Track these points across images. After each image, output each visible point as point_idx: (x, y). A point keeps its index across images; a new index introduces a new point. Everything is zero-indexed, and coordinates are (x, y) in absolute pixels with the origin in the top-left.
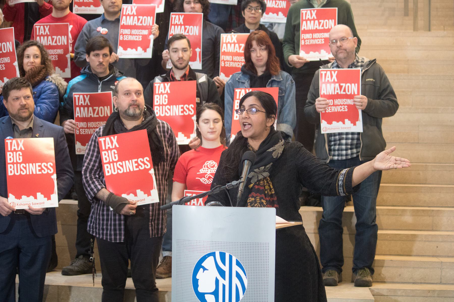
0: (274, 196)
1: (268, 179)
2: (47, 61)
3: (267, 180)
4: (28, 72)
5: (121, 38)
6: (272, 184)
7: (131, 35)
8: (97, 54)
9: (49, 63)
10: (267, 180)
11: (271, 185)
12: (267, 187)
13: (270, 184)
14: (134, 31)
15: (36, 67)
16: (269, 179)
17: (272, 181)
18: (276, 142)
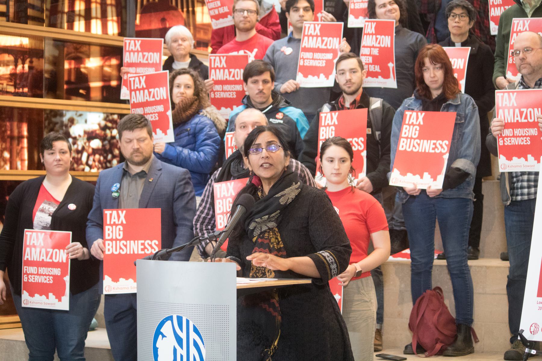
0: (283, 249)
1: (275, 230)
2: (202, 93)
3: (274, 231)
4: (178, 105)
5: (301, 63)
6: (281, 236)
7: (313, 59)
8: (255, 80)
9: (204, 95)
10: (274, 231)
11: (279, 237)
12: (273, 240)
13: (278, 236)
14: (317, 55)
15: (187, 99)
16: (277, 230)
17: (280, 232)
18: (289, 185)
